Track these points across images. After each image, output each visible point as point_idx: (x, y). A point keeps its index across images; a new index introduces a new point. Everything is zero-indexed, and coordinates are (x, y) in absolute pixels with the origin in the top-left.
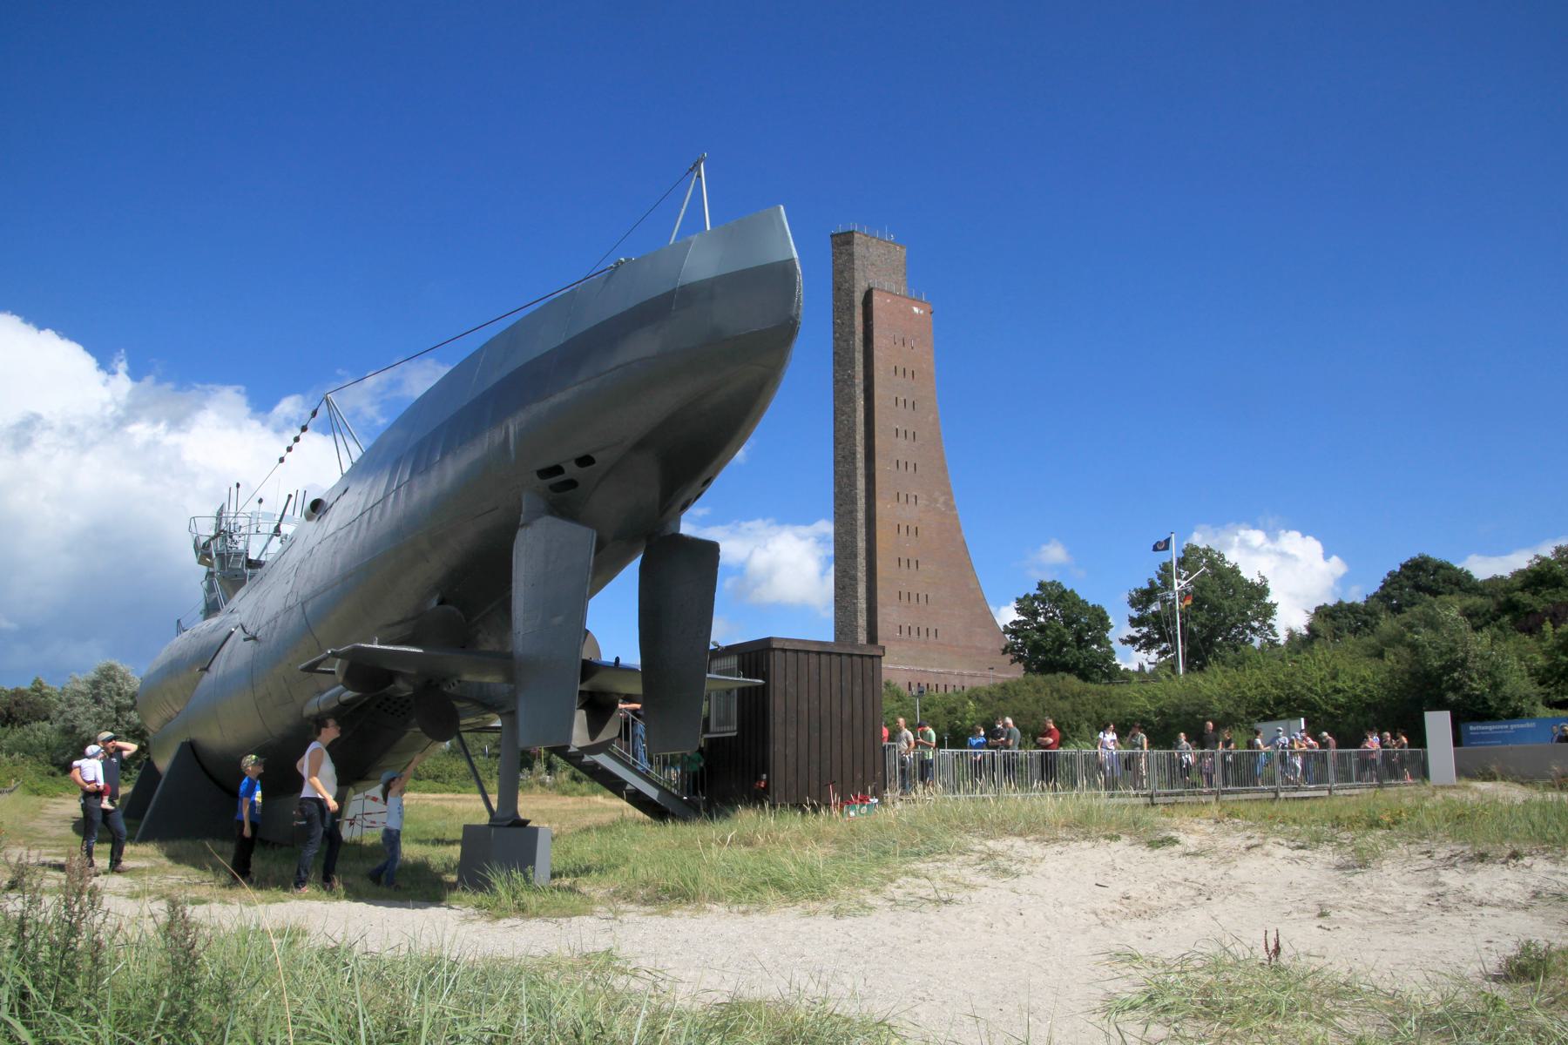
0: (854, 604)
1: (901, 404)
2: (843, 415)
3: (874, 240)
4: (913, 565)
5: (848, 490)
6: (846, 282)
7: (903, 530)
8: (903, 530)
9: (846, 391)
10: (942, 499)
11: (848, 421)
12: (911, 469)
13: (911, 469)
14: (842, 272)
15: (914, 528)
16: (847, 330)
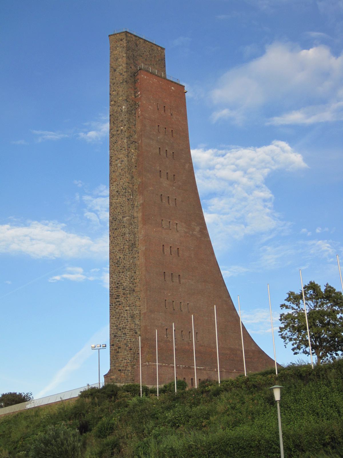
0: (126, 310)
1: (163, 153)
2: (116, 160)
3: (141, 41)
4: (176, 280)
5: (121, 217)
6: (120, 66)
7: (167, 250)
8: (167, 250)
9: (120, 142)
10: (198, 229)
11: (121, 164)
12: (172, 203)
13: (172, 203)
14: (117, 59)
15: (176, 249)
16: (121, 98)
